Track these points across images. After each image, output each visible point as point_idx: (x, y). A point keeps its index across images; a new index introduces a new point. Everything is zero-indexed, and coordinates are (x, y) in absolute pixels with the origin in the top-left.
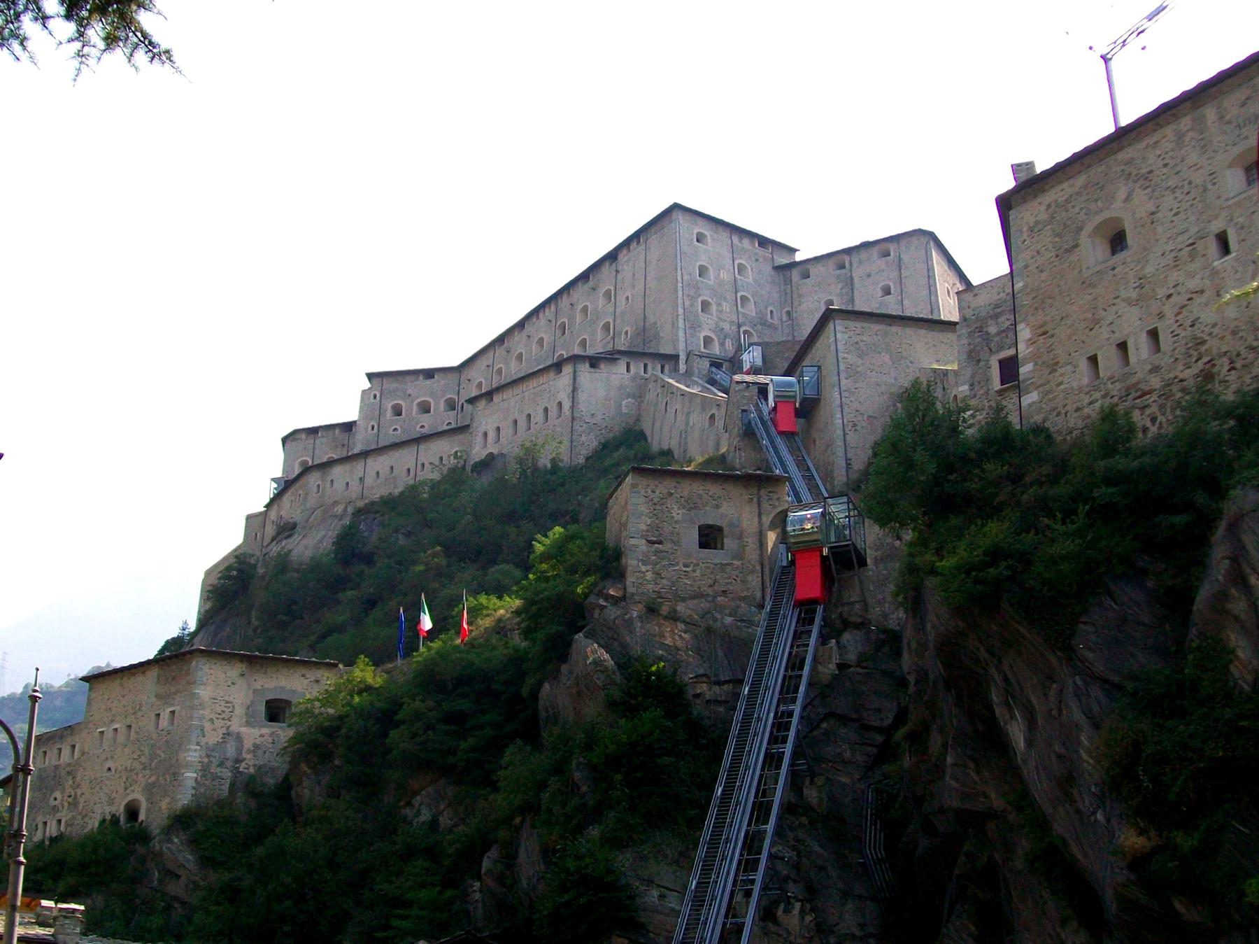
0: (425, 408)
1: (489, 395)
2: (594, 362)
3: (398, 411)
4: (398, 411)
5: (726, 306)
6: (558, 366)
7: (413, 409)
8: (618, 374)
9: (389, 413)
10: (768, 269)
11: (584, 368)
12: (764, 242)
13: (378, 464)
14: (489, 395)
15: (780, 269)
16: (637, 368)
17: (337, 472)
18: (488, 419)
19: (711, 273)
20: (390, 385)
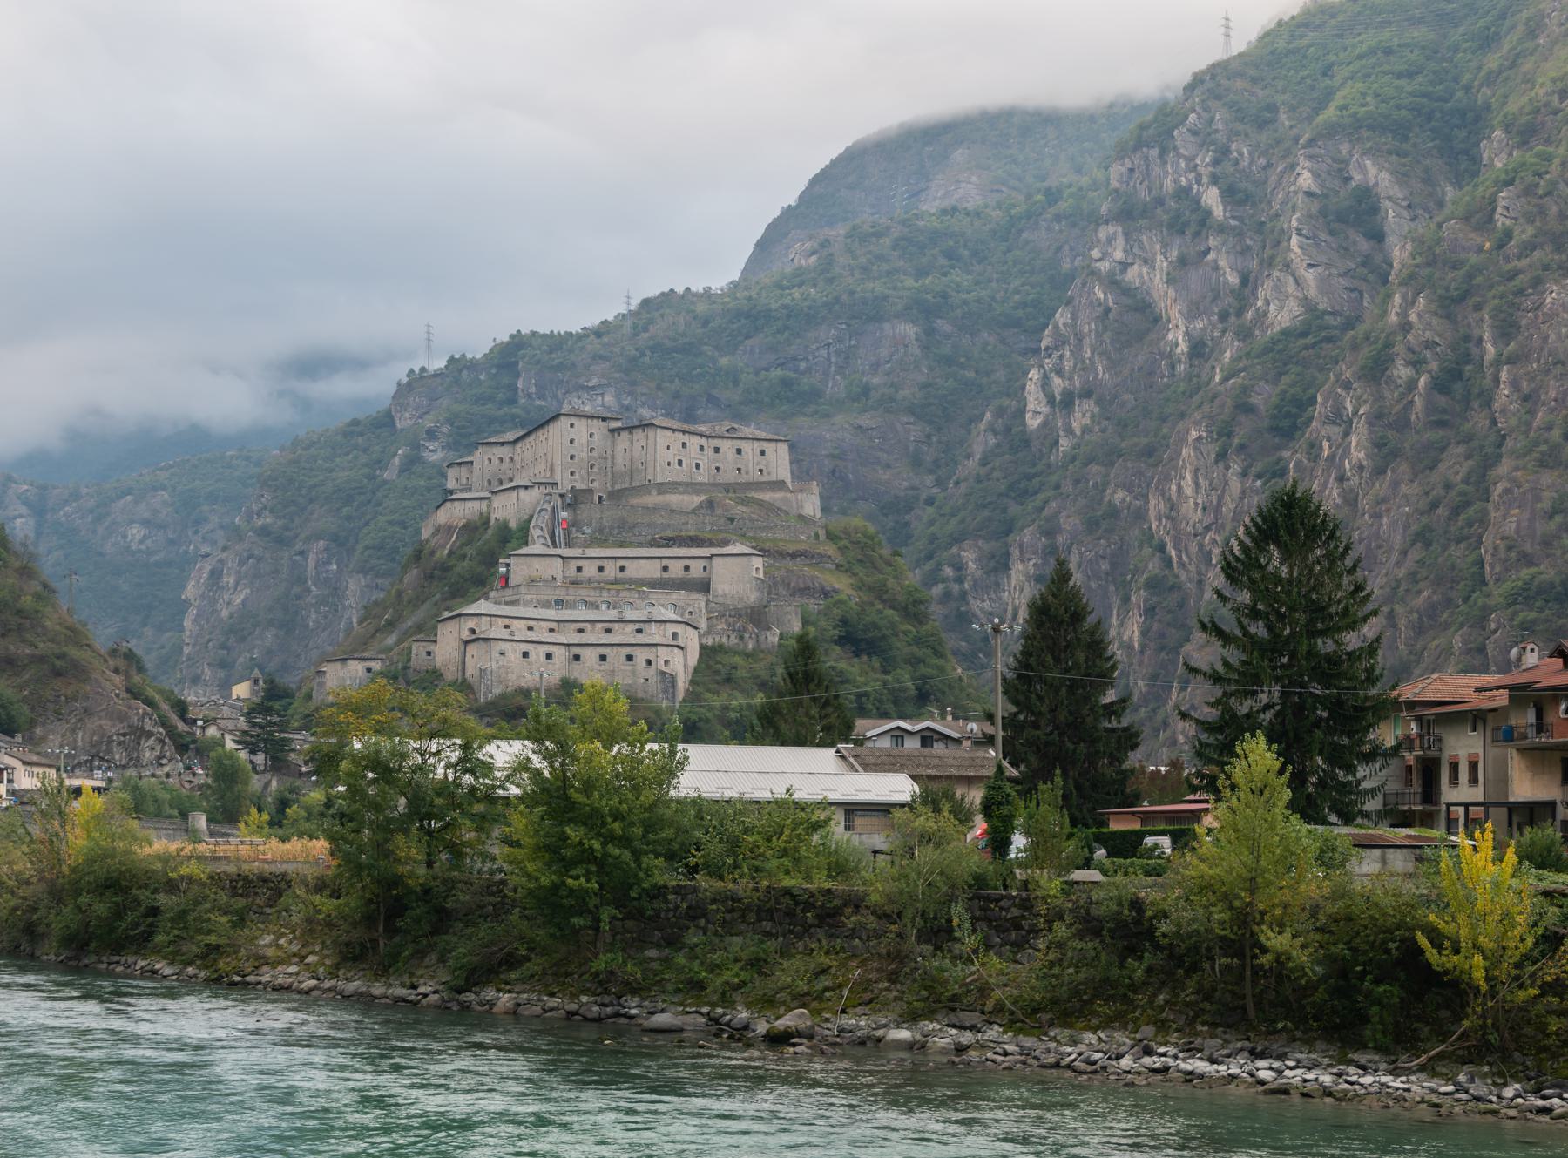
0: (501, 460)
1: (496, 492)
2: (526, 487)
3: (490, 460)
4: (490, 460)
5: (584, 455)
6: (514, 488)
7: (496, 461)
8: (536, 493)
9: (487, 462)
10: (606, 431)
11: (522, 493)
12: (604, 419)
13: (469, 504)
14: (496, 492)
15: (612, 431)
16: (542, 488)
17: (456, 503)
18: (498, 501)
19: (576, 442)
20: (486, 448)
